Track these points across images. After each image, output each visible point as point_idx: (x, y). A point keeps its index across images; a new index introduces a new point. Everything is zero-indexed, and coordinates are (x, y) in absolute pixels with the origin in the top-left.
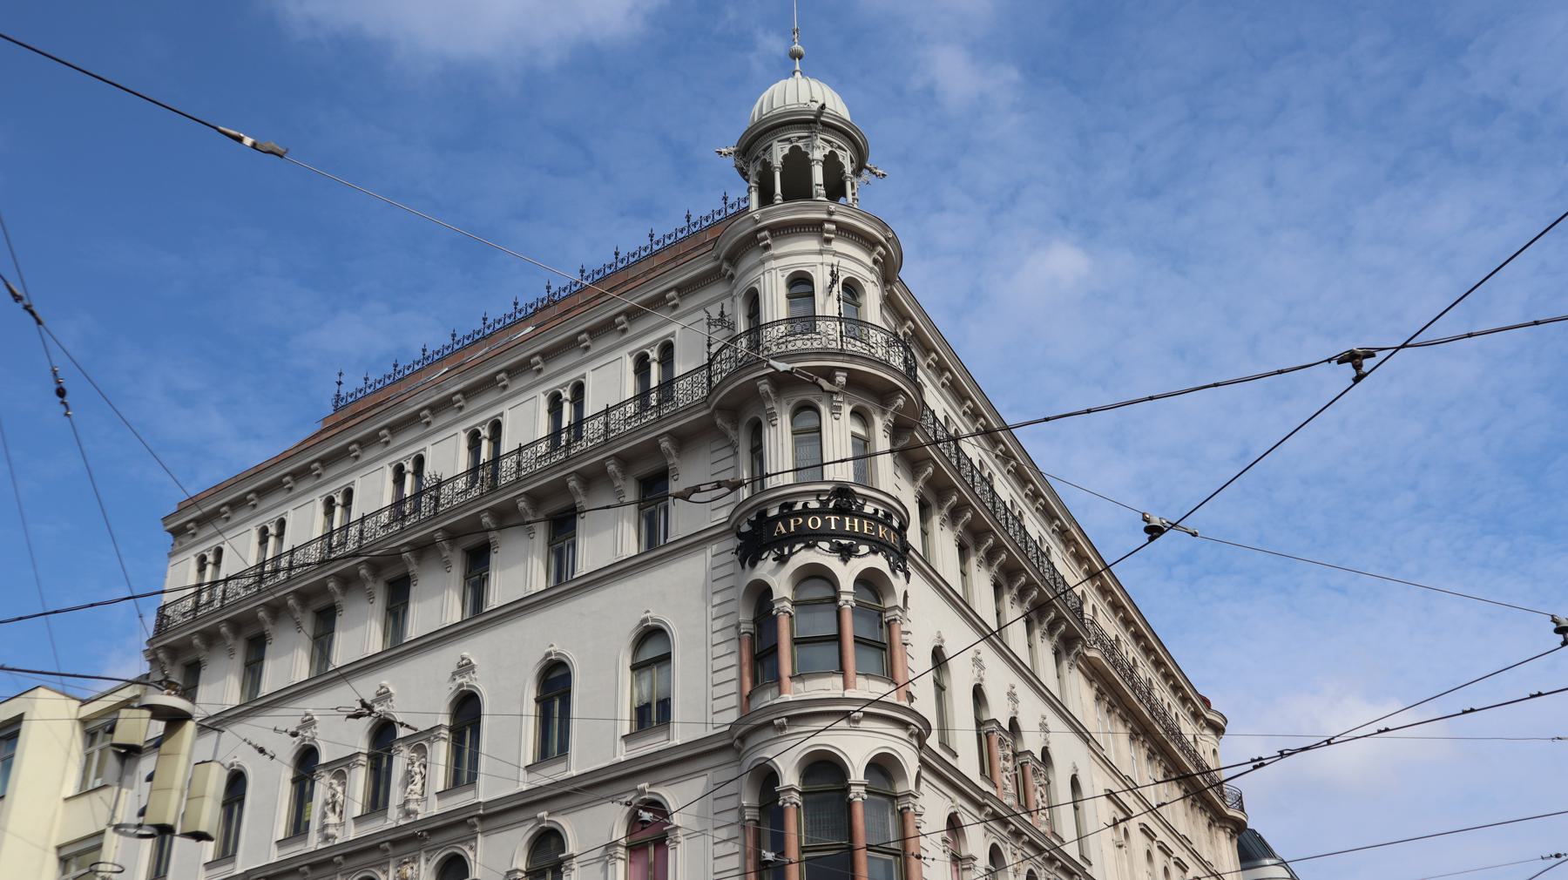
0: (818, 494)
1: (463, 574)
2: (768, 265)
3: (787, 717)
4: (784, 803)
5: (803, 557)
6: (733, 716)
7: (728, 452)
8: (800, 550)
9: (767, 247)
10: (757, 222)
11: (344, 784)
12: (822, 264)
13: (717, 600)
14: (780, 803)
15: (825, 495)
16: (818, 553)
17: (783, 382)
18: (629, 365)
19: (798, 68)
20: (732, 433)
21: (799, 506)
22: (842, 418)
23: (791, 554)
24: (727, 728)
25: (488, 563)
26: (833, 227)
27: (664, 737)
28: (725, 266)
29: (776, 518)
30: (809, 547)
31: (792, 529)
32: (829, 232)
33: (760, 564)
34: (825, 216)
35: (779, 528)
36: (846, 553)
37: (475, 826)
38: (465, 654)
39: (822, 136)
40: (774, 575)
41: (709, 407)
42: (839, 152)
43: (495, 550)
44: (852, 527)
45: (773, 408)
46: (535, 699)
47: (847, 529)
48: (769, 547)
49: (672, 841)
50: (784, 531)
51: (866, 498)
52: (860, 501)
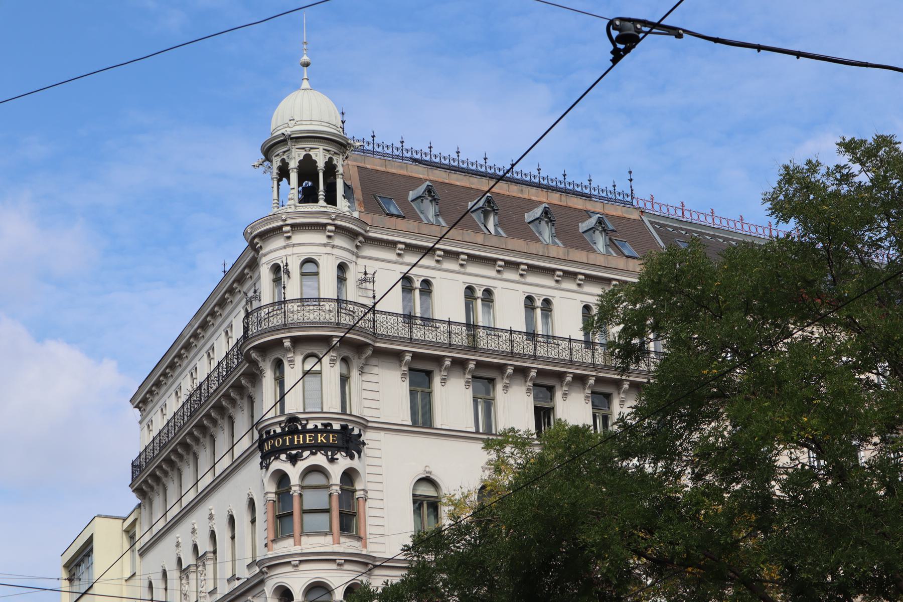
0: (280, 423)
3: (267, 567)
5: (275, 465)
9: (261, 247)
11: (188, 583)
17: (263, 349)
21: (272, 433)
22: (296, 366)
26: (288, 228)
30: (277, 458)
32: (288, 232)
34: (281, 223)
36: (293, 460)
42: (312, 153)
44: (298, 441)
47: (296, 443)
51: (307, 420)
52: (304, 422)
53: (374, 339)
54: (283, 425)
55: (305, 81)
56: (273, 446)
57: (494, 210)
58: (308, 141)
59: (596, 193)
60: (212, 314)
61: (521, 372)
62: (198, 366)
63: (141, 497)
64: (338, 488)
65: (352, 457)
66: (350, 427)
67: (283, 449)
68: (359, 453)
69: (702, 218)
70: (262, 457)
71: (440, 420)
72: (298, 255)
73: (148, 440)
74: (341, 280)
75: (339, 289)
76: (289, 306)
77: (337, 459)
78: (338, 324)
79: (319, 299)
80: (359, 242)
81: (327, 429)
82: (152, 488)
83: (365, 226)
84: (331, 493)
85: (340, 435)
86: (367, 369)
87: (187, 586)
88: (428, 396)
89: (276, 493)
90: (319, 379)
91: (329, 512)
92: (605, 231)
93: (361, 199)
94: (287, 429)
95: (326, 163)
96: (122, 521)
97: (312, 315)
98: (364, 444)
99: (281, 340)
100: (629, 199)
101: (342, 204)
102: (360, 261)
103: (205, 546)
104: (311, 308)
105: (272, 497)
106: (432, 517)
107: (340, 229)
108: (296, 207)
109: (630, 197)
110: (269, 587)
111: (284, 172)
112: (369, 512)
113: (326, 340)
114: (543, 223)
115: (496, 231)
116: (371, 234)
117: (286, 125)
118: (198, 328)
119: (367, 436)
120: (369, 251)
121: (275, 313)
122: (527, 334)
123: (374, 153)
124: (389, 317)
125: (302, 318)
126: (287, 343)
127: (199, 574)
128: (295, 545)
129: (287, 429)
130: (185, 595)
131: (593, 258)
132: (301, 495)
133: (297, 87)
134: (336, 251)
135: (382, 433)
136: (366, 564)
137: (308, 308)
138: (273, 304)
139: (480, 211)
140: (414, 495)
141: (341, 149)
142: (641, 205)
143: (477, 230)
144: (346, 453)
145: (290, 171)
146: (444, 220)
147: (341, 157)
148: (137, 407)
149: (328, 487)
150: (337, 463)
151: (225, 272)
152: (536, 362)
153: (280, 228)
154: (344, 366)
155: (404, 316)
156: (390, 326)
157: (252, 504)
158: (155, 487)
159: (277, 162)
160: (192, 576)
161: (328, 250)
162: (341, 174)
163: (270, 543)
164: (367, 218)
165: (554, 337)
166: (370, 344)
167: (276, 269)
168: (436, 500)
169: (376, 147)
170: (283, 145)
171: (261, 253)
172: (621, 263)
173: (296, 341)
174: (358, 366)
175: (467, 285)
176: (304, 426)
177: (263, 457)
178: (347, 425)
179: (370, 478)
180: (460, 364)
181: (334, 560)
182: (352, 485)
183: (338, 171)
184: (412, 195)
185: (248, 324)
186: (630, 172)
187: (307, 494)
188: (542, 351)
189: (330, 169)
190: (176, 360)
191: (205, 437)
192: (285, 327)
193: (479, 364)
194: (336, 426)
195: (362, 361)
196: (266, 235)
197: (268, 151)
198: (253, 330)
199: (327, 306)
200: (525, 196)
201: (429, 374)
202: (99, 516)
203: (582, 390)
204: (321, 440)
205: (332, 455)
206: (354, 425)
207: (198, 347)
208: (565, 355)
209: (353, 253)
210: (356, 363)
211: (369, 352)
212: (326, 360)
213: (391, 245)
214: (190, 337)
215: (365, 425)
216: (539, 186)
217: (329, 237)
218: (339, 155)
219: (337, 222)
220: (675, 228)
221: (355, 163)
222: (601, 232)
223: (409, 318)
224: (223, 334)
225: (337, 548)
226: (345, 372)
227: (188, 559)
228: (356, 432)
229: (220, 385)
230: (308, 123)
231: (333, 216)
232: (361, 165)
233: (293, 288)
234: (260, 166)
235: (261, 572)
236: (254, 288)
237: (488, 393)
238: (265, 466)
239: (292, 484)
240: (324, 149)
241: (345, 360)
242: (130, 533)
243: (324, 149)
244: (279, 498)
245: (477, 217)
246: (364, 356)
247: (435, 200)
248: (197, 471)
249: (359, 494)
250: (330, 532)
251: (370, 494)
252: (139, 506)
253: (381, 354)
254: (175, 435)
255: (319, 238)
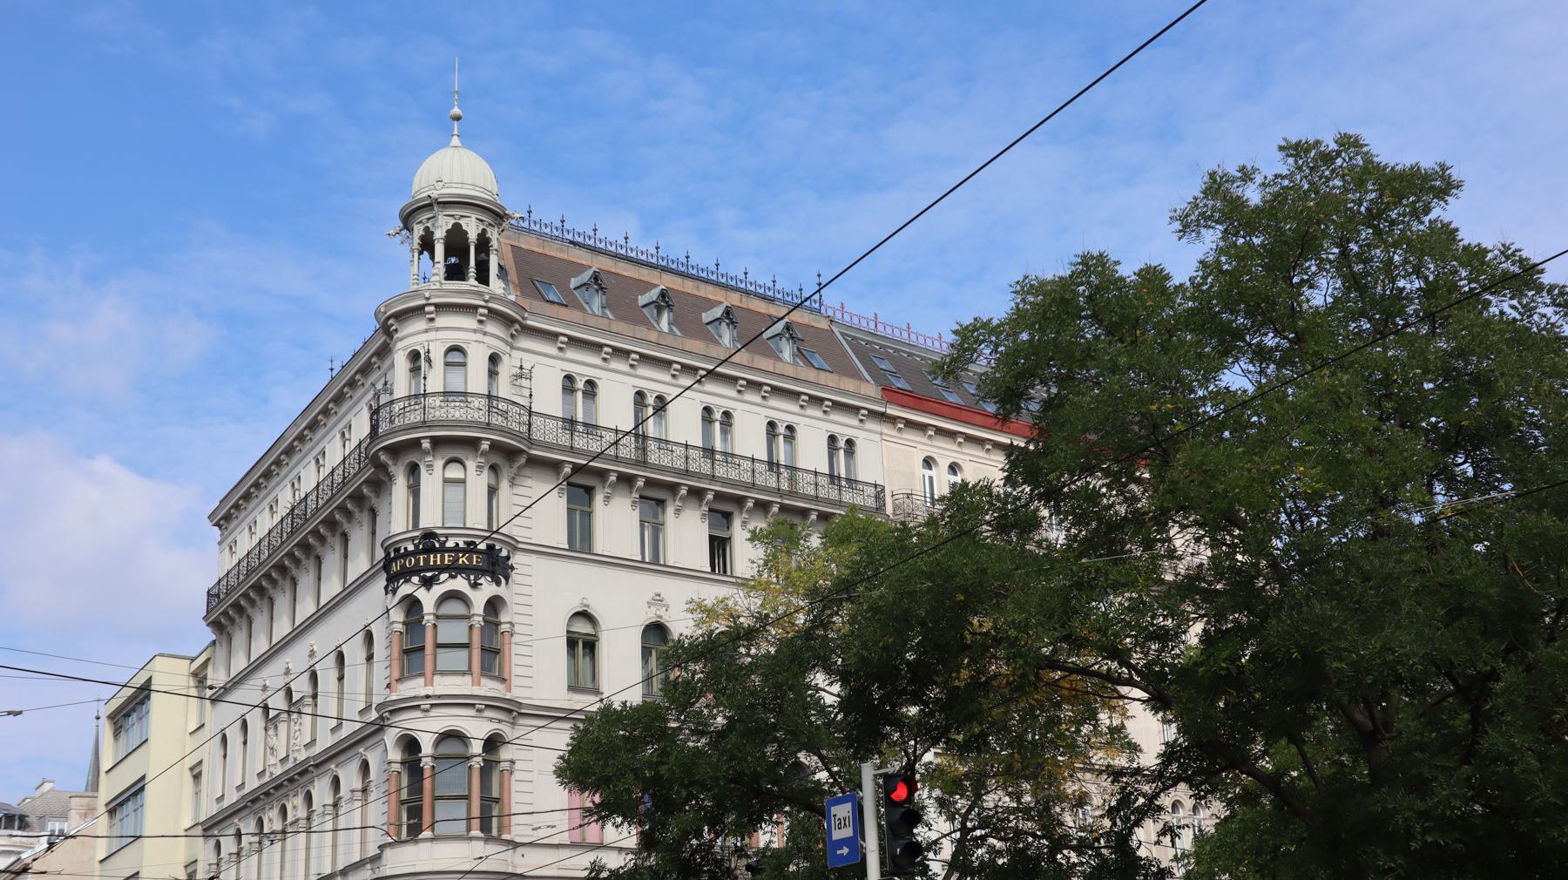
0: (413, 539)
3: (389, 711)
5: (405, 589)
9: (396, 330)
11: (277, 735)
17: (395, 451)
19: (456, 132)
21: (402, 551)
22: (435, 473)
23: (398, 587)
30: (408, 581)
32: (431, 313)
34: (424, 302)
39: (445, 213)
42: (462, 222)
44: (435, 561)
47: (432, 563)
51: (447, 536)
52: (443, 539)
53: (529, 445)
54: (416, 542)
55: (456, 137)
56: (403, 566)
57: (669, 306)
58: (461, 208)
59: (780, 296)
60: (325, 412)
61: (697, 494)
62: (302, 475)
63: (217, 633)
64: (481, 619)
65: (498, 583)
66: (497, 548)
67: (416, 571)
68: (507, 578)
69: (897, 333)
70: (387, 580)
71: (601, 545)
72: (443, 341)
73: (229, 562)
74: (493, 374)
75: (490, 384)
76: (430, 400)
77: (481, 584)
78: (488, 424)
79: (465, 394)
80: (516, 331)
81: (470, 548)
82: (232, 621)
83: (522, 311)
84: (472, 625)
85: (486, 556)
86: (518, 480)
87: (275, 738)
88: (588, 516)
89: (404, 623)
90: (461, 489)
91: (468, 647)
92: (793, 338)
93: (517, 282)
94: (421, 546)
95: (479, 235)
96: (189, 661)
97: (457, 412)
98: (512, 568)
99: (418, 440)
100: (817, 306)
101: (496, 285)
102: (514, 353)
103: (301, 687)
104: (457, 404)
105: (399, 627)
106: (588, 659)
107: (494, 314)
108: (441, 284)
109: (818, 304)
110: (391, 736)
111: (427, 244)
112: (515, 649)
113: (473, 443)
114: (724, 324)
115: (671, 329)
116: (529, 323)
117: (432, 187)
118: (305, 429)
119: (517, 560)
120: (526, 343)
121: (412, 407)
122: (704, 449)
123: (529, 231)
124: (547, 420)
125: (445, 416)
126: (426, 444)
127: (292, 723)
128: (425, 686)
129: (421, 546)
130: (272, 749)
131: (779, 368)
132: (435, 626)
133: (446, 144)
134: (487, 339)
135: (534, 557)
136: (510, 711)
137: (453, 404)
138: (409, 397)
139: (653, 306)
140: (568, 632)
141: (496, 220)
142: (830, 313)
143: (650, 327)
144: (492, 578)
145: (436, 242)
146: (610, 311)
147: (496, 229)
148: (217, 524)
149: (468, 617)
150: (481, 589)
151: (332, 370)
152: (713, 482)
153: (422, 308)
154: (492, 475)
155: (564, 420)
156: (548, 432)
157: (369, 638)
158: (237, 620)
159: (418, 231)
160: (283, 727)
161: (479, 337)
162: (496, 250)
163: (394, 683)
164: (525, 303)
165: (733, 455)
166: (525, 451)
167: (415, 356)
168: (592, 638)
169: (532, 225)
170: (427, 211)
171: (395, 337)
172: (811, 375)
173: (437, 442)
174: (508, 476)
175: (638, 389)
177: (390, 580)
178: (494, 545)
179: (517, 609)
180: (626, 480)
181: (473, 705)
182: (497, 615)
183: (492, 246)
184: (574, 282)
185: (378, 420)
186: (819, 276)
187: (443, 626)
188: (720, 471)
189: (483, 244)
190: (273, 467)
191: (308, 558)
192: (424, 425)
193: (650, 483)
194: (482, 546)
195: (514, 470)
196: (402, 316)
197: (408, 219)
198: (383, 427)
199: (476, 402)
200: (701, 294)
201: (589, 491)
202: (161, 655)
203: (763, 518)
204: (463, 561)
205: (475, 579)
206: (502, 545)
207: (304, 451)
208: (747, 477)
209: (507, 343)
210: (506, 473)
211: (523, 460)
212: (471, 465)
213: (552, 336)
214: (294, 440)
215: (514, 546)
216: (717, 284)
217: (481, 322)
218: (494, 226)
219: (490, 305)
220: (868, 342)
221: (507, 241)
222: (788, 340)
223: (570, 423)
224: (338, 436)
225: (476, 691)
226: (493, 482)
227: (278, 702)
228: (504, 553)
229: (333, 495)
230: (460, 186)
231: (487, 297)
232: (514, 243)
233: (435, 380)
234: (397, 235)
235: (381, 718)
236: (383, 379)
237: (656, 517)
238: (390, 589)
239: (425, 611)
240: (477, 219)
241: (494, 468)
242: (199, 677)
243: (477, 219)
244: (407, 630)
245: (649, 313)
246: (517, 465)
247: (602, 288)
248: (295, 600)
249: (504, 627)
250: (469, 672)
251: (517, 629)
252: (214, 642)
253: (536, 463)
254: (270, 556)
255: (469, 322)
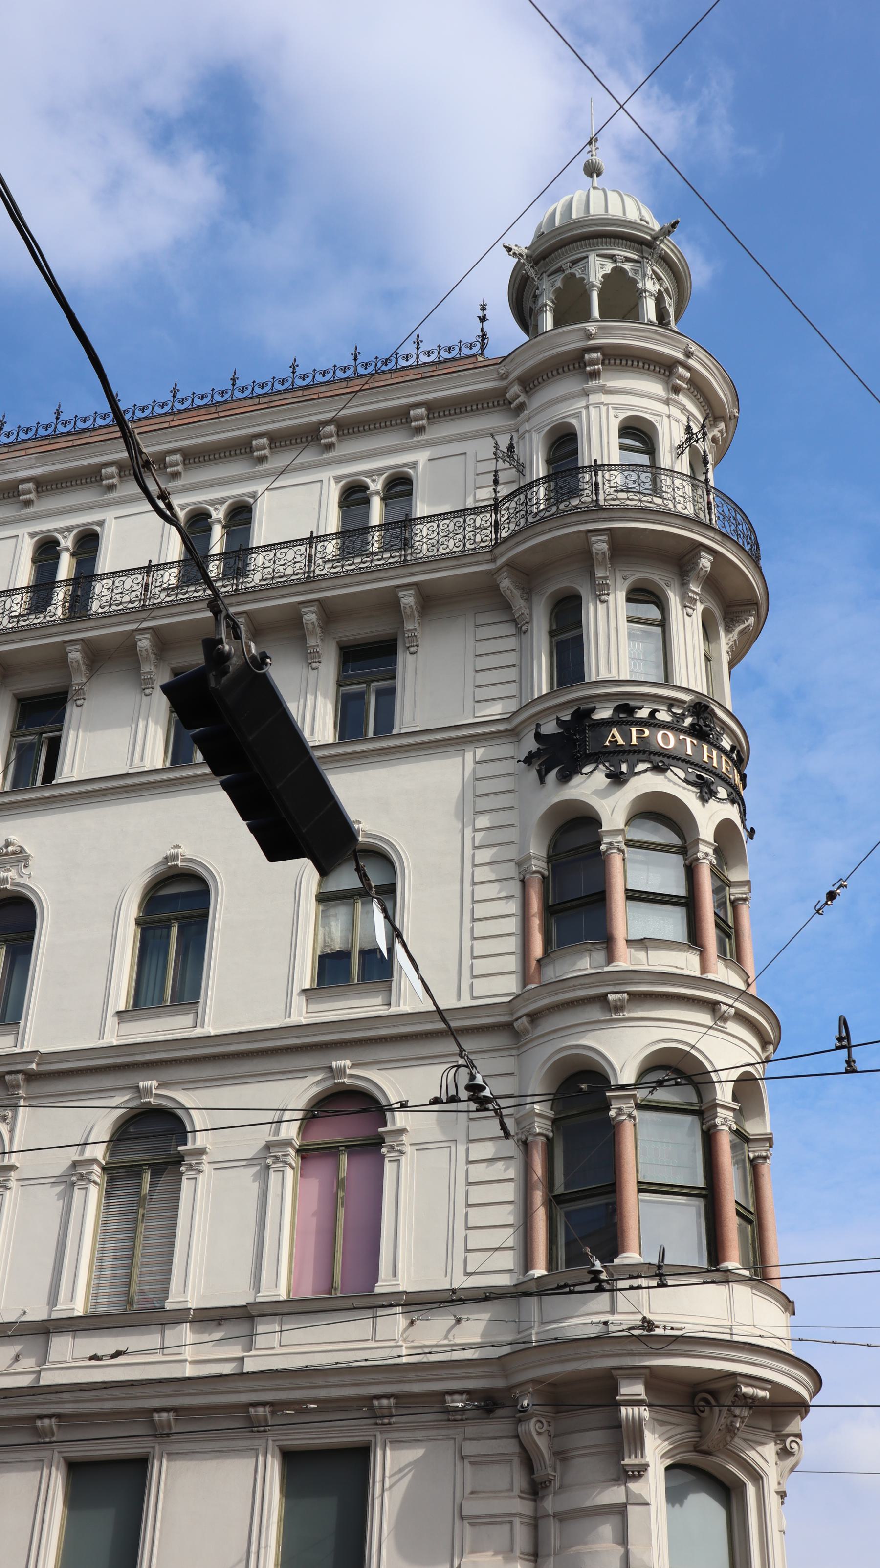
0: (671, 703)
1: (9, 729)
2: (594, 398)
3: (628, 993)
4: (618, 1115)
6: (510, 985)
7: (508, 629)
8: (645, 771)
9: (595, 375)
10: (589, 336)
12: (669, 416)
13: (483, 821)
14: (612, 1113)
15: (680, 707)
16: (670, 781)
18: (334, 493)
20: (519, 604)
21: (643, 714)
24: (508, 999)
25: (61, 719)
27: (379, 1000)
28: (516, 389)
29: (607, 724)
31: (634, 741)
33: (577, 780)
34: (681, 357)
35: (613, 736)
37: (18, 1087)
38: (15, 838)
40: (603, 798)
41: (493, 560)
43: (79, 702)
45: (606, 578)
46: (136, 919)
48: (597, 757)
49: (392, 1149)
50: (621, 741)
176: (719, 737)
